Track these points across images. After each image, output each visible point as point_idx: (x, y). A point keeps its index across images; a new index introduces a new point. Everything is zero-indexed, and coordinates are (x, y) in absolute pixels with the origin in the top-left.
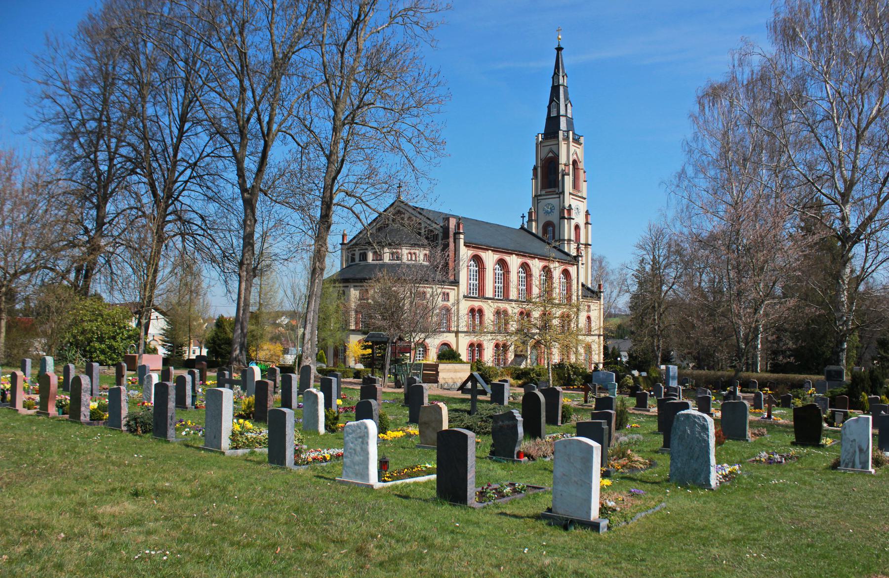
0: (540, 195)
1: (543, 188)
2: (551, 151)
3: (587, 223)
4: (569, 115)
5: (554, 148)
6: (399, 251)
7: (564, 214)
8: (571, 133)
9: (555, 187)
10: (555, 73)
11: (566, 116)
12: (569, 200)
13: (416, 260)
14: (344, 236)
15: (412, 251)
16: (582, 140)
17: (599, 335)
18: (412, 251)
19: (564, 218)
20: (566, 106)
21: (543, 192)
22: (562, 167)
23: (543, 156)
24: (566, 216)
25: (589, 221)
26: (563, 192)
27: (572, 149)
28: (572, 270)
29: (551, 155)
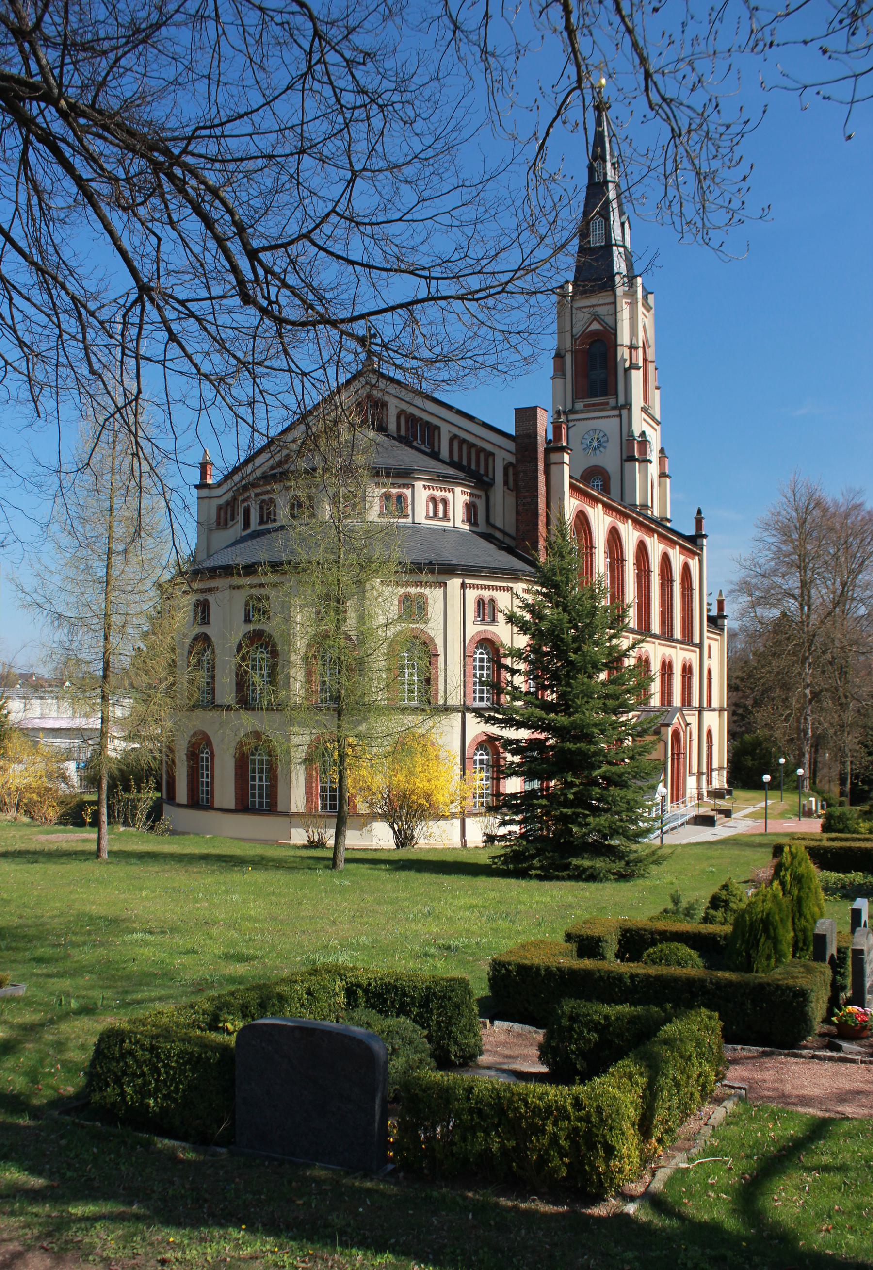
0: (573, 411)
1: (577, 396)
2: (596, 318)
3: (663, 475)
4: (628, 244)
5: (602, 311)
6: (408, 492)
7: (632, 451)
8: (639, 280)
9: (605, 393)
10: (595, 158)
11: (624, 247)
12: (639, 424)
13: (446, 517)
14: (204, 467)
15: (438, 494)
16: (651, 298)
17: (721, 710)
18: (438, 494)
19: (632, 459)
20: (622, 224)
21: (579, 406)
22: (623, 353)
23: (578, 329)
24: (637, 455)
25: (667, 472)
26: (628, 406)
27: (640, 317)
28: (694, 564)
29: (595, 326)
